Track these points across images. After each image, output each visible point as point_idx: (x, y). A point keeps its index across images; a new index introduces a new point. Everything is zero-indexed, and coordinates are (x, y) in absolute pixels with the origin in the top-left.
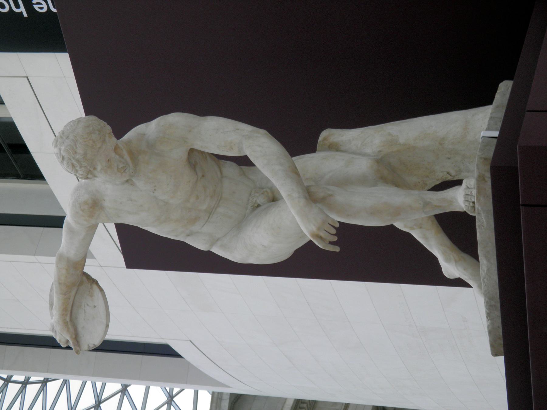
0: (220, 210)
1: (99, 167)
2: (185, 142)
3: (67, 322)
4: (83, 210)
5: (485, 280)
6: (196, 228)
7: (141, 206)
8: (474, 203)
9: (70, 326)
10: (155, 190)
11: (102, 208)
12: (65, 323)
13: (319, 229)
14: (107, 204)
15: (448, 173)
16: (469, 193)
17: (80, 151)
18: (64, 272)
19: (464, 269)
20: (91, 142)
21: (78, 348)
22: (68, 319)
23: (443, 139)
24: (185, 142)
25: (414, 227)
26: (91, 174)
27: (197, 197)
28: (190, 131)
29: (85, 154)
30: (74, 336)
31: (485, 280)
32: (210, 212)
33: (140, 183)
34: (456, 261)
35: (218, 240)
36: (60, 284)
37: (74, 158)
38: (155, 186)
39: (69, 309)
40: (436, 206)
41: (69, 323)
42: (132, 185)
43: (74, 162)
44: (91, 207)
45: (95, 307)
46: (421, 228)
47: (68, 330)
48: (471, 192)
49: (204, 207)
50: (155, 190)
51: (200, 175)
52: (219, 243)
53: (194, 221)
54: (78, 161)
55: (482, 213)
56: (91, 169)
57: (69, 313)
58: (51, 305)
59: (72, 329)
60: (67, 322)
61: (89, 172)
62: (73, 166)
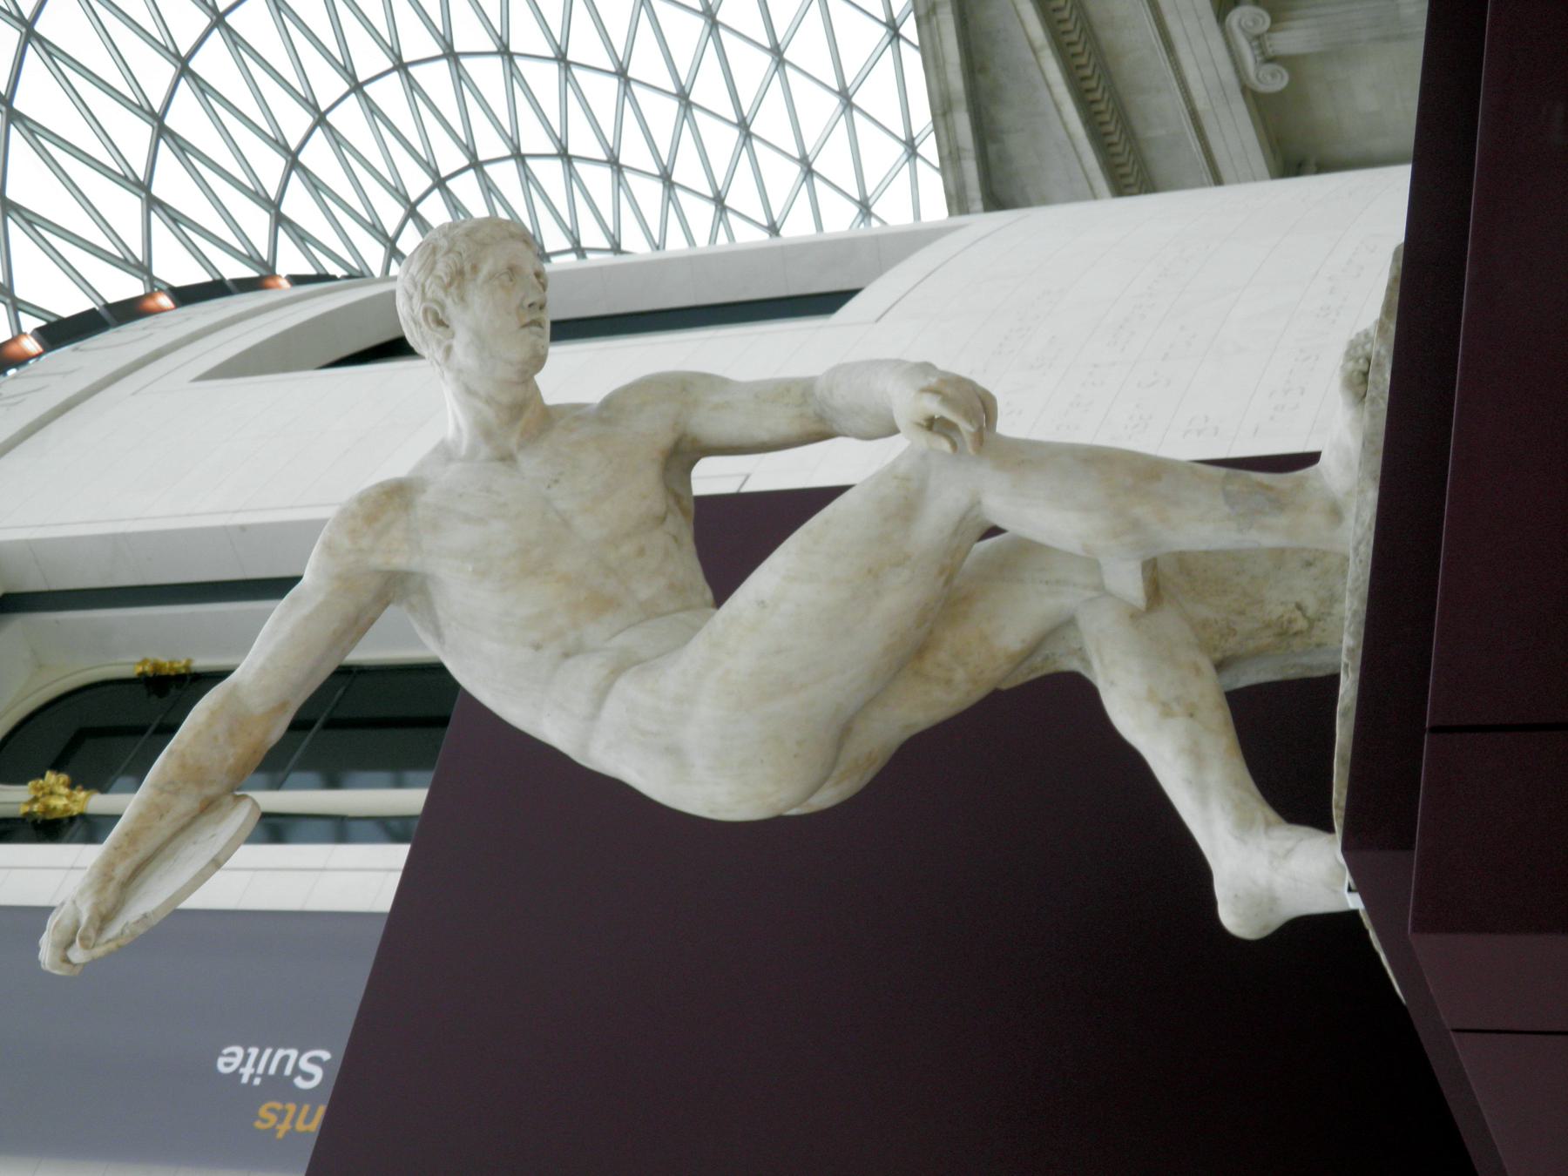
1: (485, 269)
3: (111, 879)
9: (112, 887)
10: (556, 481)
11: (407, 506)
14: (428, 498)
15: (1299, 607)
21: (92, 934)
22: (121, 871)
26: (459, 287)
27: (641, 552)
30: (103, 909)
32: (650, 612)
33: (531, 464)
34: (1268, 825)
38: (561, 474)
46: (1191, 715)
47: (102, 889)
53: (601, 604)
56: (467, 268)
57: (137, 858)
60: (111, 879)
61: (460, 273)
62: (434, 250)
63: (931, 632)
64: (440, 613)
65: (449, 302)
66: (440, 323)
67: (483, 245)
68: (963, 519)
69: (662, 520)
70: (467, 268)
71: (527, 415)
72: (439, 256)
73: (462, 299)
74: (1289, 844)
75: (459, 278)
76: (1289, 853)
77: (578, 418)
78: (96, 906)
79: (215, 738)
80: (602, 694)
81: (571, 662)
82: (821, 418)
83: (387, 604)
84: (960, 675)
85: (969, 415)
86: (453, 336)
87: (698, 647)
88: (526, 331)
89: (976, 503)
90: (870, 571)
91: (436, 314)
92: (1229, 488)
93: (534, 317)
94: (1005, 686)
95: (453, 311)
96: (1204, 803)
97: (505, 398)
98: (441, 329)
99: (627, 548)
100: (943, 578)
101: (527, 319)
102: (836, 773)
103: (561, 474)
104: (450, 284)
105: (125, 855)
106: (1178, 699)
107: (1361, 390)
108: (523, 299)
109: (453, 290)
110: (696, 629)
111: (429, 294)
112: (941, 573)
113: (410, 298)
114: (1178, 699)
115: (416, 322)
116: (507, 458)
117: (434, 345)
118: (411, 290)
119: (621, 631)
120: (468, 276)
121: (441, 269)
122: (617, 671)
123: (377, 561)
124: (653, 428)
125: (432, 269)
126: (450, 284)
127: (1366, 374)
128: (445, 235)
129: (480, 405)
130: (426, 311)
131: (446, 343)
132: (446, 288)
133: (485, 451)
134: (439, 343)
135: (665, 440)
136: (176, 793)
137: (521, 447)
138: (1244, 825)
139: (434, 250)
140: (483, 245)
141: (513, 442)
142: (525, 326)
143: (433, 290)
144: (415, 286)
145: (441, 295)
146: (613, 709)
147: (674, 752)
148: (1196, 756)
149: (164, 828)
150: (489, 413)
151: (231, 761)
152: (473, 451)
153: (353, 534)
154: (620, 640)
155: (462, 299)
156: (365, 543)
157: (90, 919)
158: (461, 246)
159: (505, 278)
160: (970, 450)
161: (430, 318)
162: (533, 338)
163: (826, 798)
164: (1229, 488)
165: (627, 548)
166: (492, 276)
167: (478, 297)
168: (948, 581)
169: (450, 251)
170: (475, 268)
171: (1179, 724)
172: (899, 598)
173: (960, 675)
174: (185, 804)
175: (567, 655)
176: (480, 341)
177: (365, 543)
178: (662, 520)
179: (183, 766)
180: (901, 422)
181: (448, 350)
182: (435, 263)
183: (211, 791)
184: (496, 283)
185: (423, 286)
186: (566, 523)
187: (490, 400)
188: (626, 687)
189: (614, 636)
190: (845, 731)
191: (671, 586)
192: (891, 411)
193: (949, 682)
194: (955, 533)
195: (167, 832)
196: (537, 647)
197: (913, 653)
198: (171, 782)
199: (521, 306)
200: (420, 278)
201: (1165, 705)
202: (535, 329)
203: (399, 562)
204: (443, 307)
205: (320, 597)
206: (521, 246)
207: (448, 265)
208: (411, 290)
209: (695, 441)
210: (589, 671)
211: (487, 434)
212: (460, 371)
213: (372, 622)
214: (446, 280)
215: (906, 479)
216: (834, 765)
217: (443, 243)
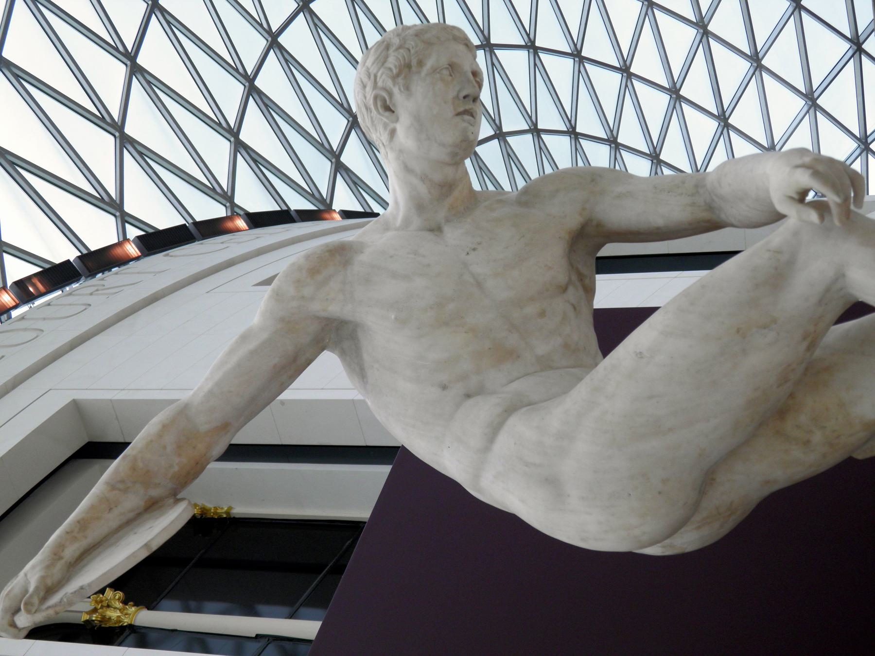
1: (429, 64)
3: (61, 558)
7: (429, 265)
9: (60, 565)
10: (474, 250)
11: (346, 263)
21: (36, 601)
22: (70, 552)
24: (593, 180)
27: (542, 314)
30: (49, 582)
32: (545, 364)
33: (453, 235)
35: (530, 404)
38: (479, 244)
41: (62, 562)
44: (330, 251)
49: (542, 348)
50: (474, 250)
53: (503, 354)
56: (414, 62)
57: (84, 543)
60: (61, 558)
61: (408, 66)
62: (388, 47)
63: (792, 396)
64: (366, 357)
65: (396, 90)
66: (388, 109)
67: (429, 44)
68: (828, 290)
69: (564, 289)
70: (414, 62)
71: (456, 193)
72: (391, 51)
73: (407, 88)
75: (406, 71)
77: (500, 201)
78: (43, 578)
79: (165, 448)
80: (495, 429)
81: (471, 402)
82: (710, 207)
83: (323, 350)
84: (817, 437)
85: (836, 188)
86: (397, 120)
87: (581, 392)
89: (840, 276)
90: (738, 331)
91: (385, 101)
93: (467, 107)
94: (860, 456)
95: (399, 97)
97: (437, 177)
98: (387, 114)
99: (530, 310)
100: (805, 345)
101: (461, 109)
102: (698, 517)
103: (479, 244)
104: (398, 75)
105: (75, 539)
108: (459, 91)
109: (400, 80)
110: (580, 379)
111: (380, 84)
112: (804, 338)
115: (367, 108)
116: (436, 230)
117: (380, 128)
118: (365, 80)
119: (518, 378)
120: (414, 69)
121: (392, 62)
122: (510, 410)
123: (316, 307)
124: (566, 214)
125: (383, 64)
126: (398, 75)
128: (398, 35)
129: (416, 181)
130: (376, 98)
131: (392, 126)
132: (394, 78)
133: (417, 222)
134: (385, 126)
135: (574, 221)
136: (125, 491)
137: (448, 221)
139: (388, 47)
140: (429, 44)
141: (441, 215)
142: (458, 114)
143: (384, 80)
144: (369, 77)
145: (389, 83)
146: (504, 442)
147: (552, 483)
149: (112, 520)
150: (423, 189)
151: (176, 468)
152: (407, 223)
153: (299, 283)
154: (515, 386)
155: (407, 88)
156: (307, 291)
157: (37, 588)
159: (446, 72)
160: (837, 223)
161: (379, 104)
162: (465, 125)
163: (687, 541)
165: (530, 310)
166: (434, 70)
167: (419, 88)
168: (811, 347)
169: (400, 47)
170: (421, 63)
172: (765, 357)
173: (817, 437)
174: (132, 501)
175: (468, 396)
176: (420, 125)
177: (307, 291)
179: (134, 469)
180: (781, 208)
181: (393, 133)
182: (387, 57)
183: (155, 493)
184: (438, 76)
185: (375, 76)
186: (479, 285)
187: (424, 178)
188: (519, 426)
189: (512, 381)
190: (707, 479)
191: (566, 346)
192: (767, 191)
193: (807, 443)
194: (820, 302)
196: (444, 387)
197: (774, 412)
198: (122, 481)
199: (457, 97)
202: (467, 117)
203: (335, 309)
204: (391, 94)
205: (265, 336)
206: (462, 48)
207: (397, 58)
208: (365, 80)
209: (599, 225)
210: (483, 410)
211: (419, 206)
212: (401, 151)
213: (309, 362)
214: (395, 71)
215: (779, 252)
216: (696, 506)
217: (396, 41)
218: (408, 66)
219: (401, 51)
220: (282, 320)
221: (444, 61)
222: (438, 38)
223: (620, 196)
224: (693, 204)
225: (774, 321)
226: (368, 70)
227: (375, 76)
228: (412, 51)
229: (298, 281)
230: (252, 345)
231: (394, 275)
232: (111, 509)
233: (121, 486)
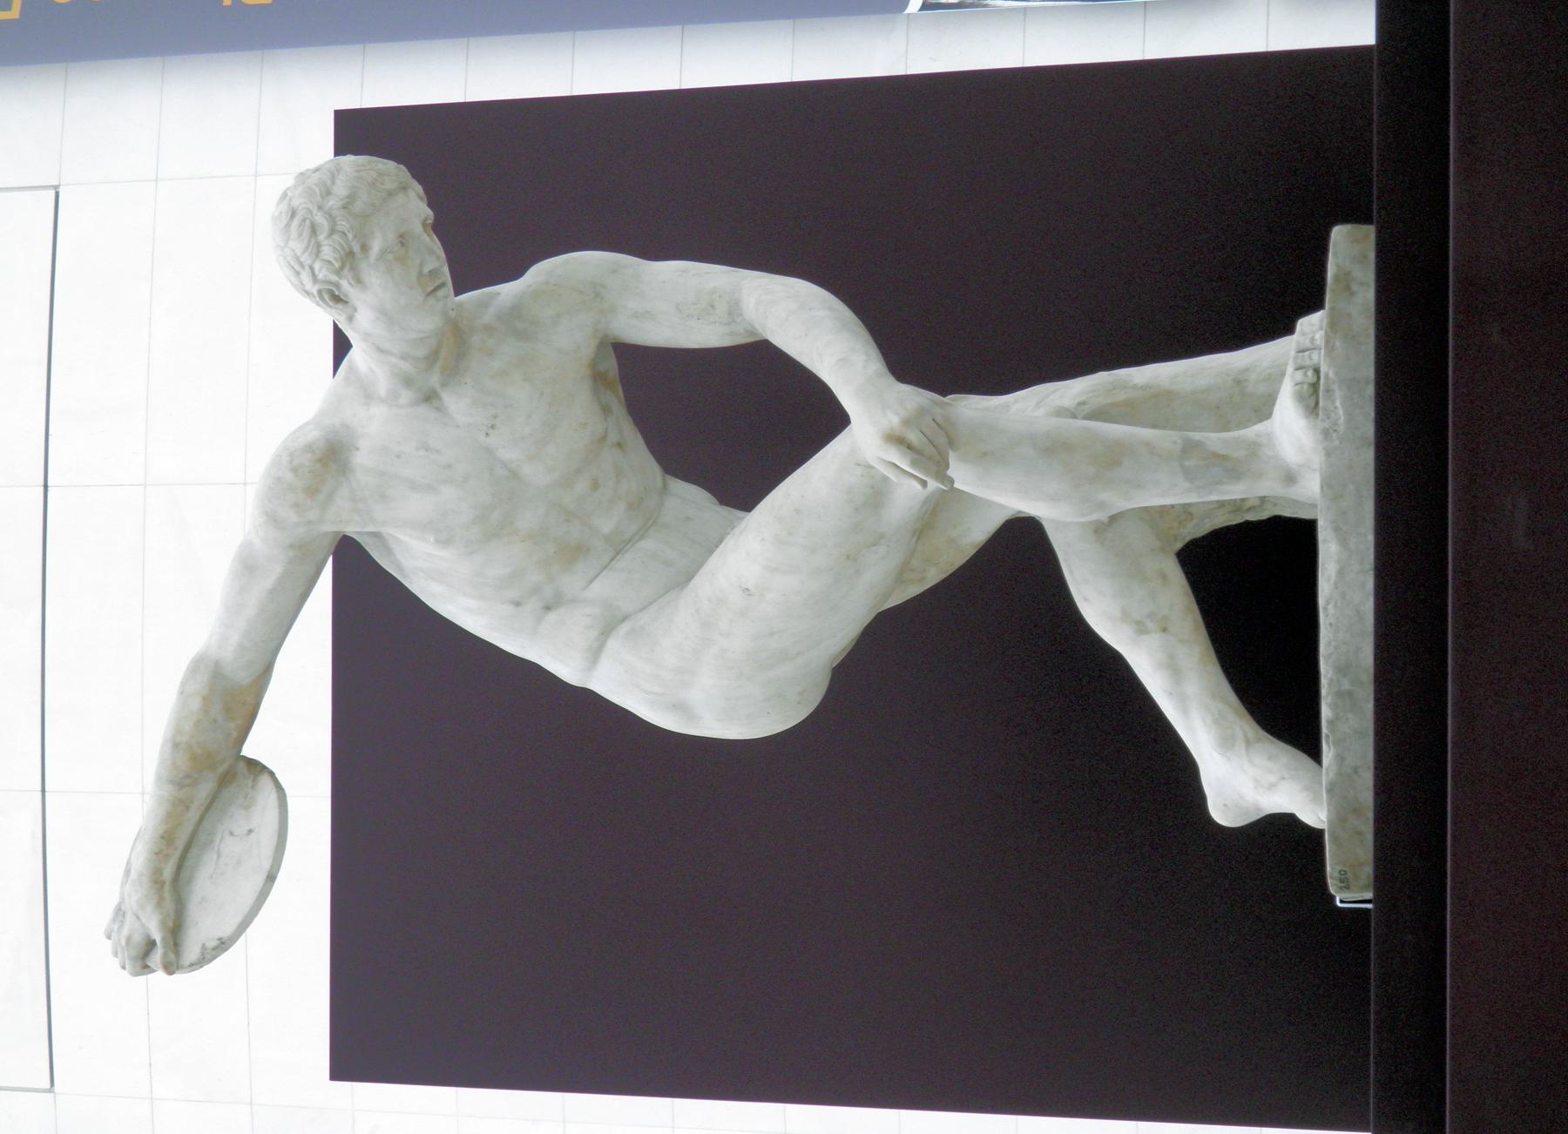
0: (647, 544)
1: (376, 246)
2: (597, 295)
3: (163, 883)
4: (295, 470)
5: (1330, 607)
6: (571, 582)
7: (449, 466)
8: (1317, 371)
9: (167, 895)
10: (493, 427)
12: (157, 881)
13: (907, 422)
14: (363, 458)
16: (1308, 344)
17: (341, 190)
18: (196, 704)
19: (1270, 758)
20: (374, 174)
21: (172, 956)
22: (168, 873)
23: (1247, 370)
25: (1150, 625)
27: (595, 486)
28: (615, 271)
29: (352, 197)
30: (171, 924)
31: (1330, 607)
32: (619, 546)
33: (457, 403)
34: (1248, 743)
35: (625, 619)
36: (176, 745)
37: (320, 208)
39: (180, 843)
40: (1216, 455)
41: (167, 887)
42: (438, 409)
43: (320, 219)
44: (320, 460)
45: (250, 831)
46: (1164, 630)
47: (159, 904)
48: (1313, 340)
49: (606, 525)
50: (493, 427)
51: (613, 437)
52: (624, 628)
53: (572, 553)
54: (330, 216)
55: (1335, 387)
56: (356, 248)
57: (177, 854)
58: (127, 872)
59: (169, 904)
60: (163, 883)
62: (314, 230)
65: (344, 284)
70: (356, 248)
72: (321, 237)
73: (358, 281)
74: (1272, 778)
75: (349, 260)
76: (1272, 786)
78: (163, 923)
79: (215, 721)
81: (552, 617)
88: (431, 300)
92: (1187, 463)
96: (1185, 712)
97: (422, 352)
98: (340, 306)
103: (495, 417)
104: (342, 268)
105: (167, 856)
106: (1151, 616)
107: (1312, 404)
108: (421, 265)
109: (346, 271)
111: (320, 276)
113: (298, 273)
114: (1151, 616)
116: (430, 397)
118: (297, 268)
120: (358, 256)
125: (318, 252)
126: (342, 268)
127: (1315, 386)
129: (394, 360)
130: (320, 292)
132: (338, 272)
133: (406, 396)
135: (588, 350)
136: (195, 783)
137: (444, 385)
138: (1226, 743)
141: (434, 379)
142: (429, 294)
144: (302, 265)
145: (334, 278)
147: (680, 707)
148: (1172, 668)
149: (193, 815)
150: (406, 366)
157: (163, 939)
158: (343, 225)
161: (326, 297)
164: (1187, 463)
165: (581, 486)
166: (383, 252)
167: (373, 277)
169: (332, 232)
170: (365, 248)
171: (1155, 639)
175: (548, 608)
176: (384, 314)
177: (312, 515)
178: (604, 438)
179: (194, 758)
182: (319, 245)
183: (222, 769)
185: (311, 268)
186: (514, 475)
187: (404, 357)
189: (591, 582)
191: (630, 506)
195: (195, 819)
196: (518, 604)
198: (187, 776)
199: (420, 274)
200: (306, 259)
201: (1138, 623)
204: (338, 286)
218: (351, 254)
219: (336, 237)
220: (292, 546)
221: (392, 236)
222: (373, 205)
223: (636, 315)
224: (732, 333)
225: (882, 536)
226: (297, 259)
227: (311, 268)
228: (350, 236)
229: (296, 505)
230: (268, 582)
231: (414, 486)
232: (188, 808)
233: (187, 782)
